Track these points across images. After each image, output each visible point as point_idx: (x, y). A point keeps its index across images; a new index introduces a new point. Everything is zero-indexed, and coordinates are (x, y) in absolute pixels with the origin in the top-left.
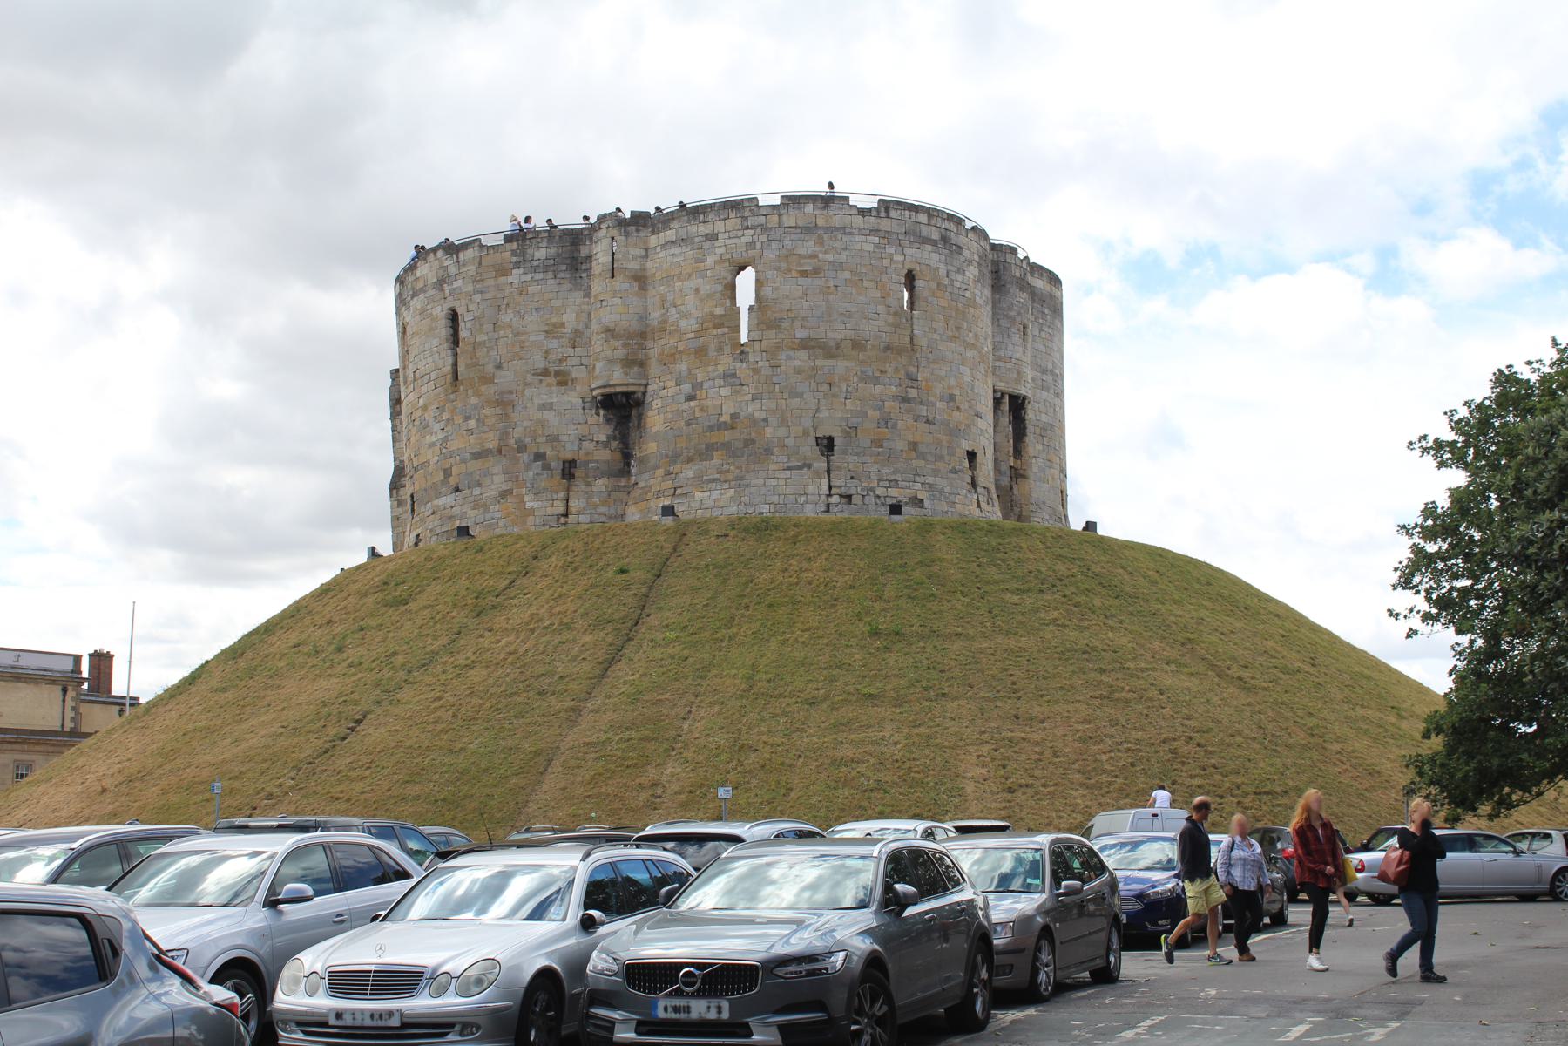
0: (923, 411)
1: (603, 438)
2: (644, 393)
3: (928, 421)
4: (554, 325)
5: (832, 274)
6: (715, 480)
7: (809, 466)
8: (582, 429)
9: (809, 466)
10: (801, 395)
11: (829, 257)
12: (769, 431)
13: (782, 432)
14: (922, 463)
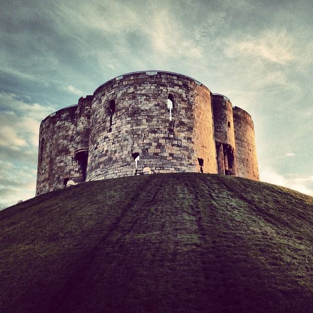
0: (176, 142)
1: (77, 169)
2: (88, 152)
3: (178, 146)
4: (66, 136)
5: (139, 98)
6: (99, 174)
7: (129, 164)
8: (72, 167)
9: (129, 164)
10: (127, 140)
11: (139, 92)
12: (117, 155)
13: (120, 154)
14: (175, 161)
